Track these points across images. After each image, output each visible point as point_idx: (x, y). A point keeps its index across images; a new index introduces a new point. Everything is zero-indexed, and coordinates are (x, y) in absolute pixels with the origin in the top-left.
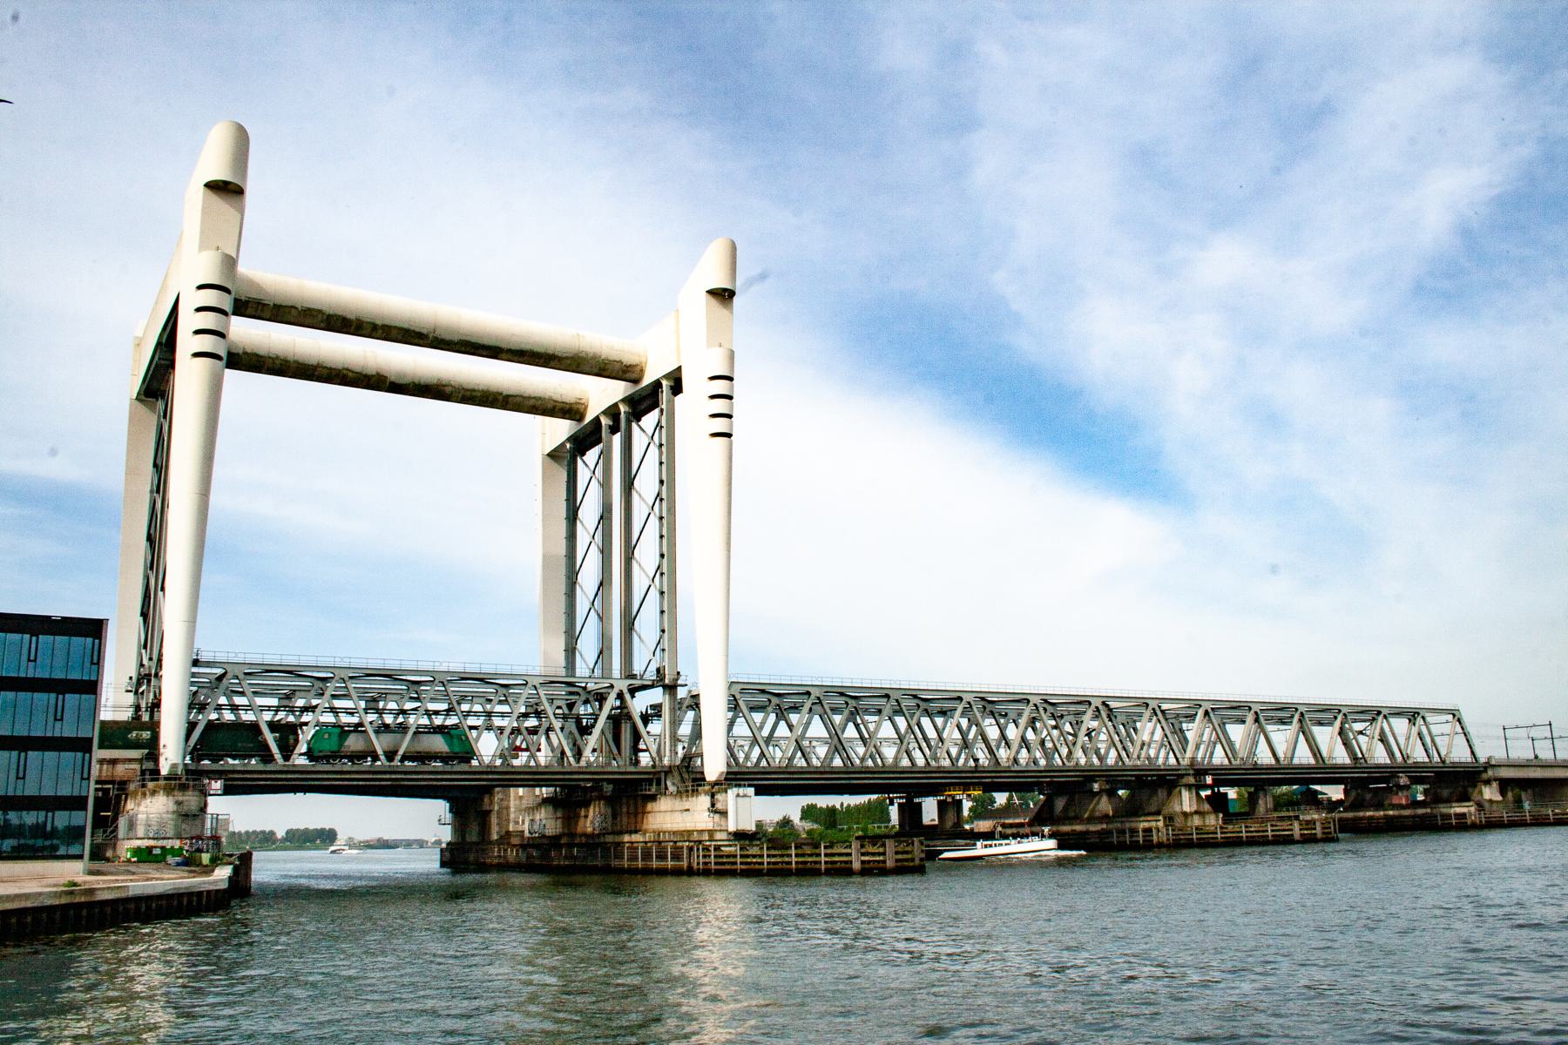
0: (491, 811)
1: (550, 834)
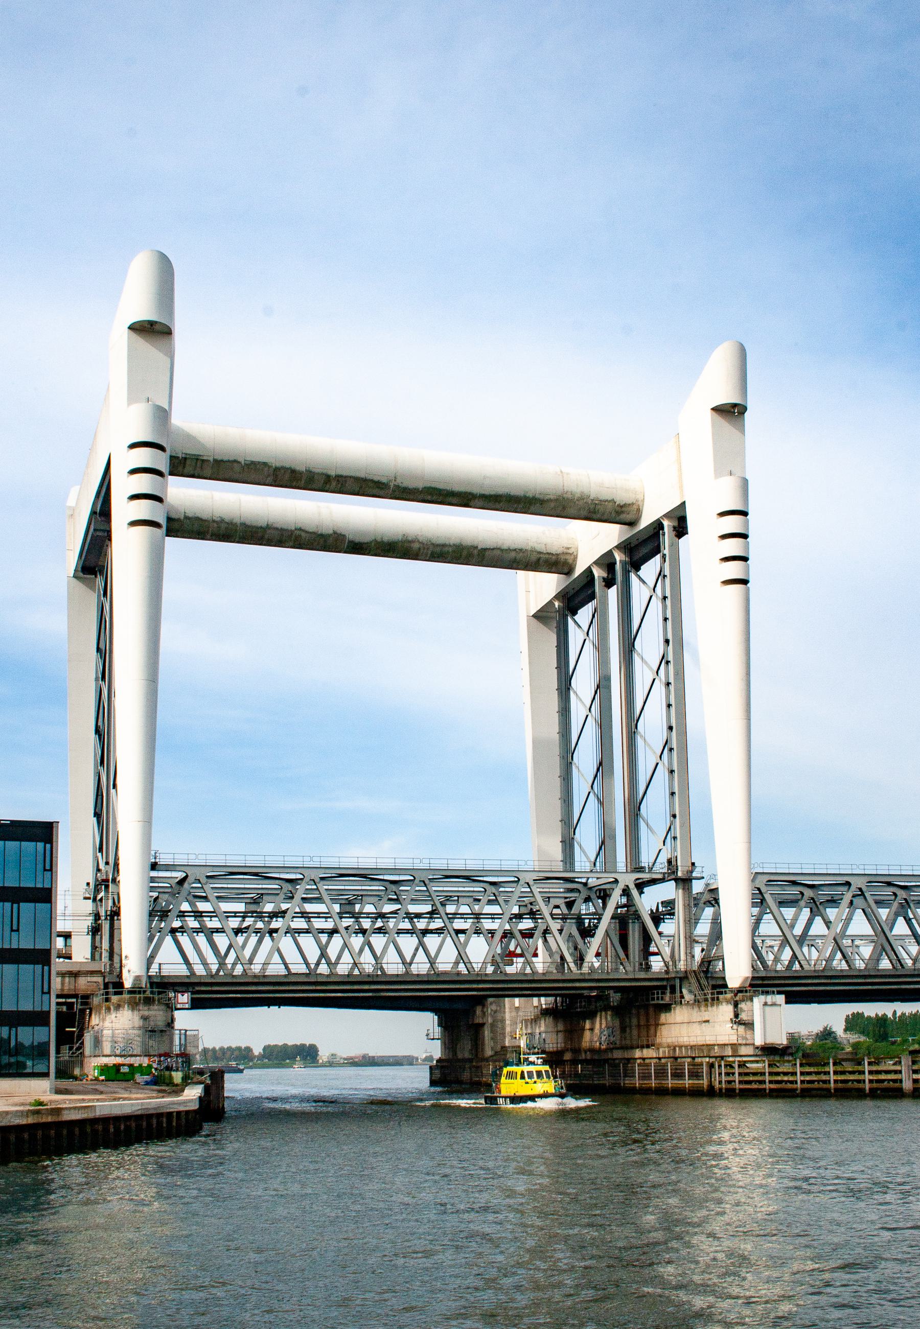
0: (483, 1025)
1: (551, 1050)
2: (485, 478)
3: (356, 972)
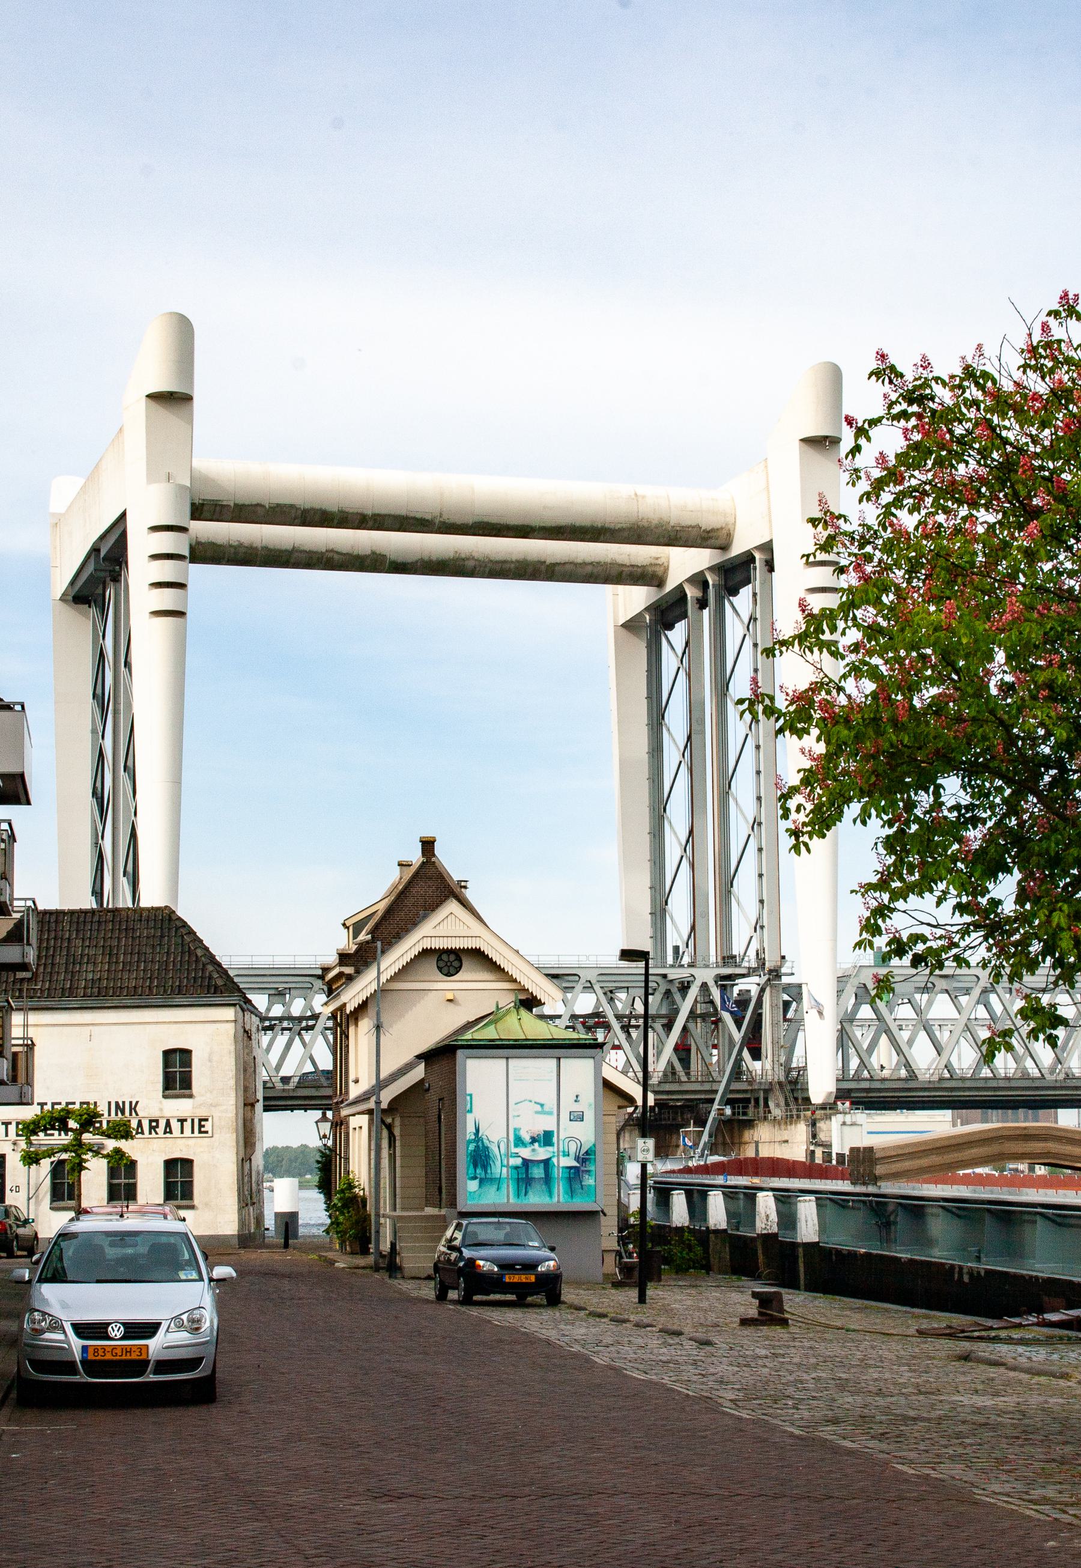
2: (544, 507)
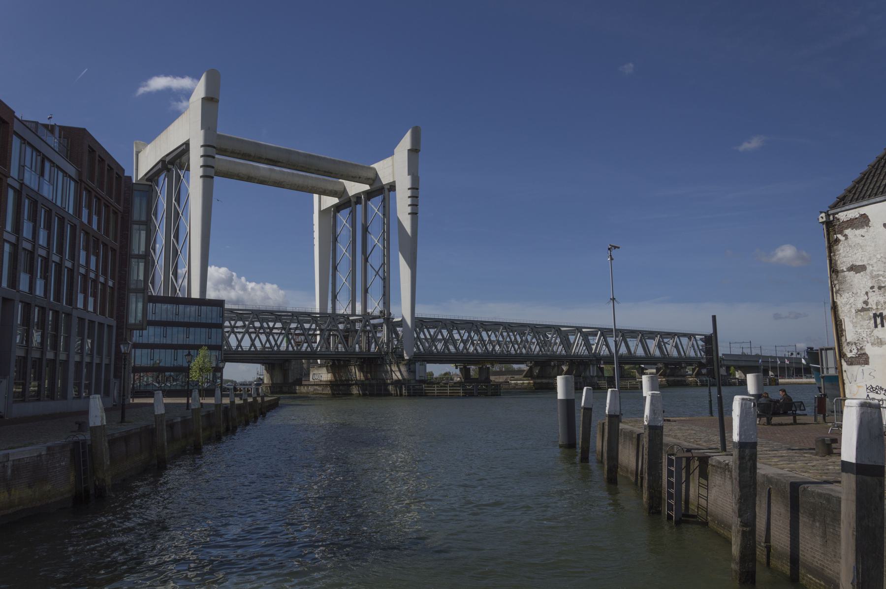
3: (240, 349)
